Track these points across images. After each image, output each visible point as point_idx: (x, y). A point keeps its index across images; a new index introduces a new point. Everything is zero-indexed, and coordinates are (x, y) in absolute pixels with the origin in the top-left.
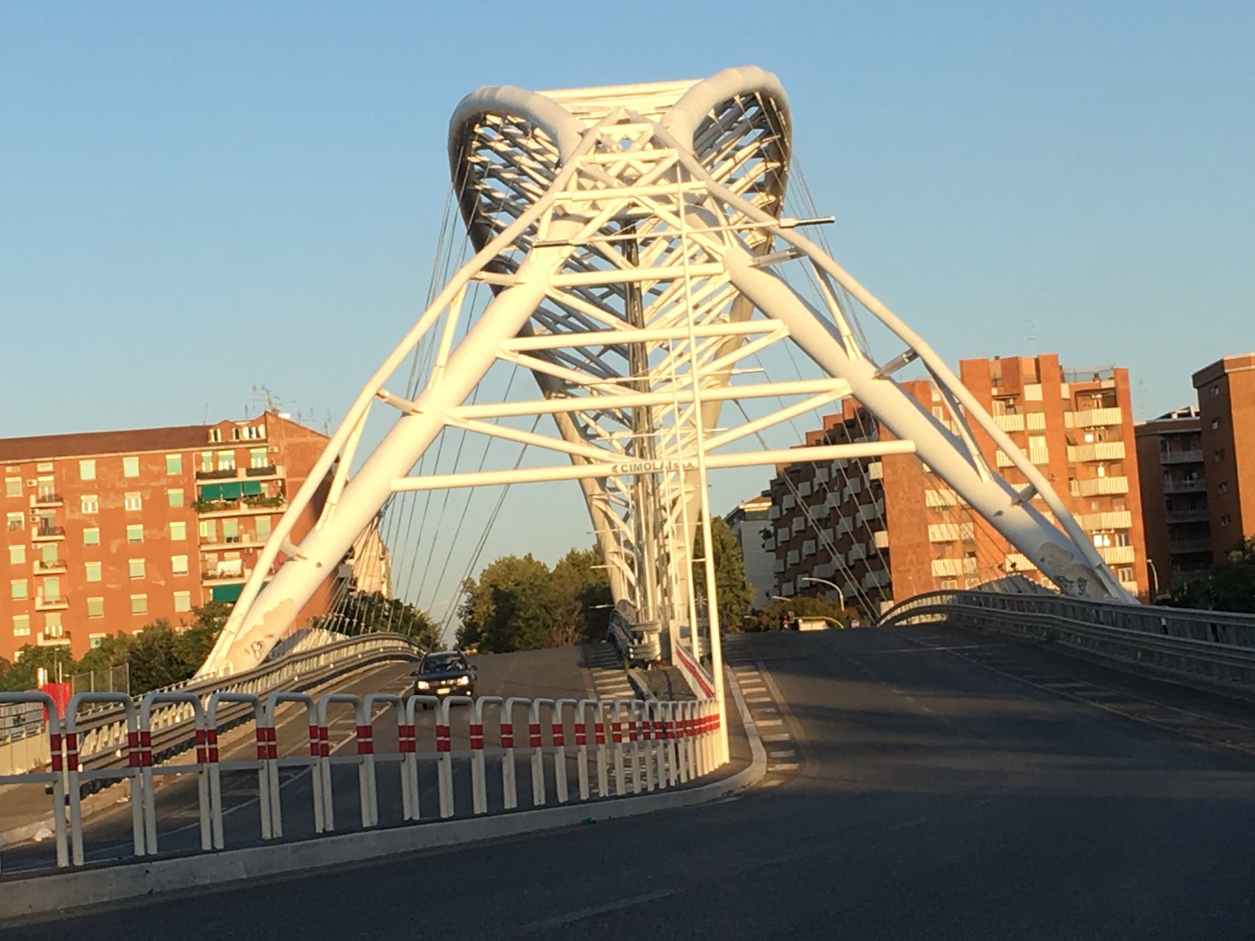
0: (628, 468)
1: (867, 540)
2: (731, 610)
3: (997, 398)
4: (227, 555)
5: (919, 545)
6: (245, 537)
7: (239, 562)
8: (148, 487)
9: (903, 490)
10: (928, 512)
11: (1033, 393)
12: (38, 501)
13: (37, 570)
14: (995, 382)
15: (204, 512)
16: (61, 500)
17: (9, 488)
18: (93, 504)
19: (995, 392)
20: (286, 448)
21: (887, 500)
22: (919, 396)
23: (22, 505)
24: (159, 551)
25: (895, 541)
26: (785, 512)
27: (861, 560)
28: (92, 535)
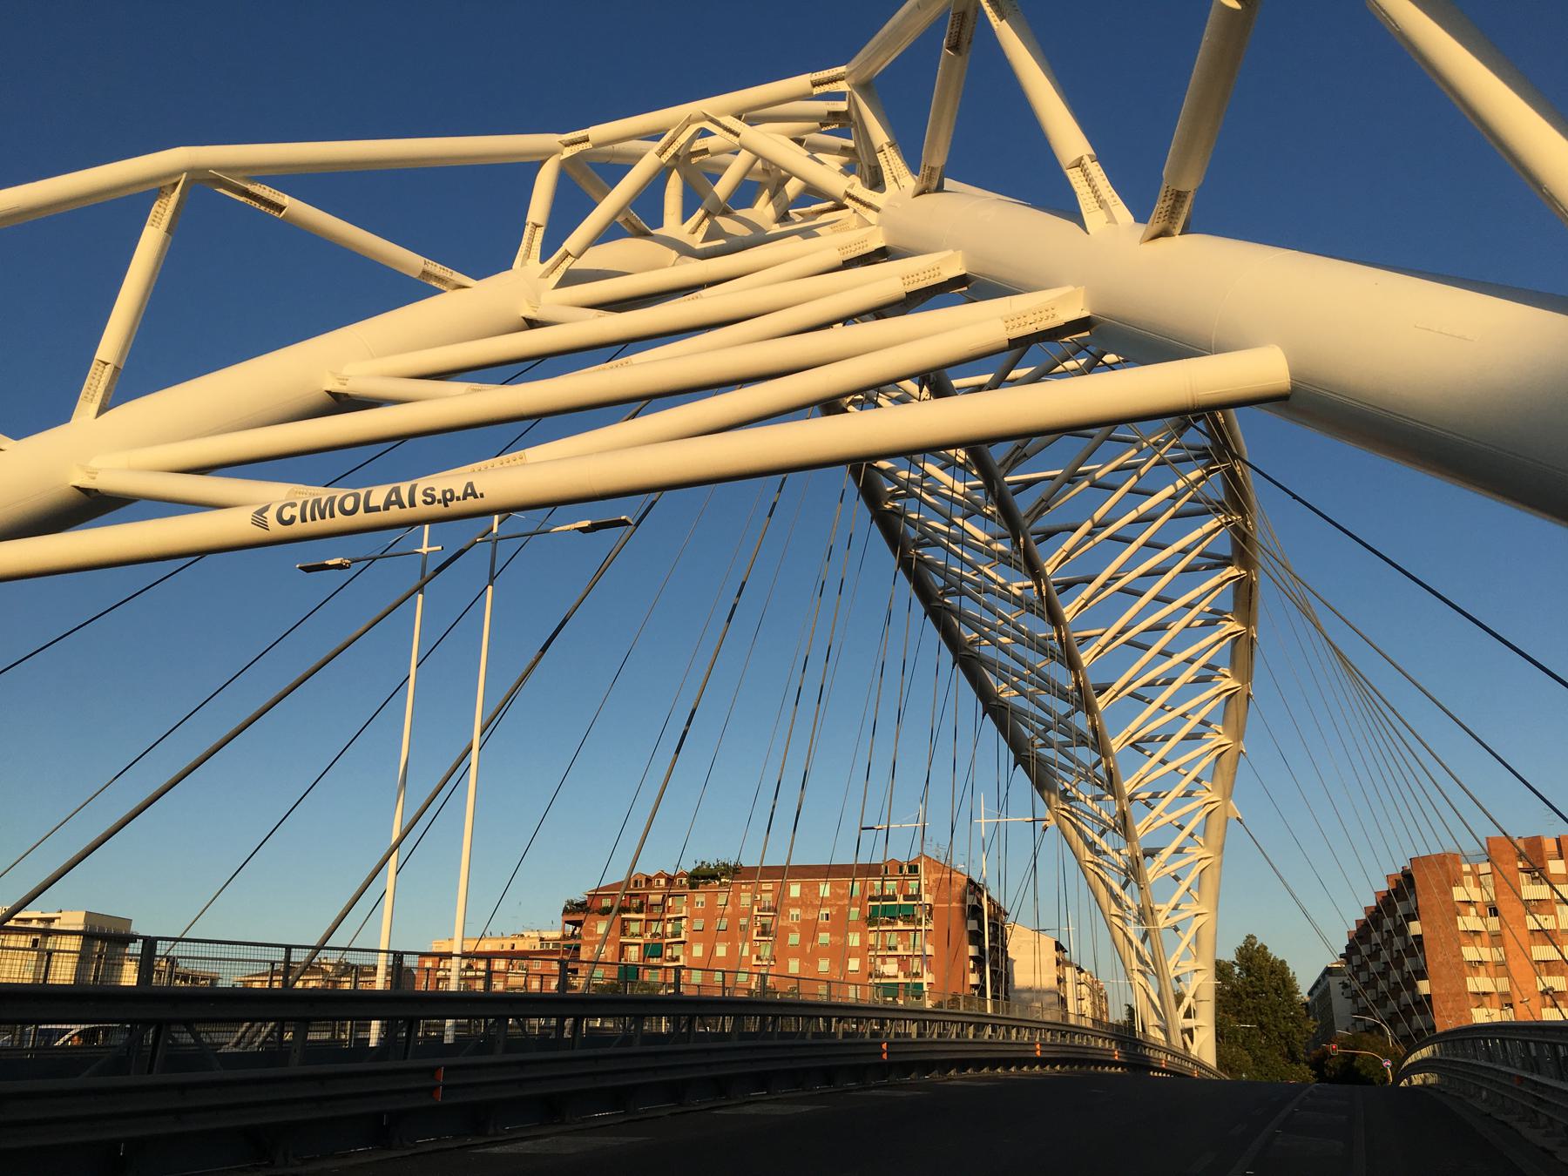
0: (297, 512)
1: (1413, 987)
2: (1293, 1039)
3: (1523, 870)
4: (888, 960)
5: (1458, 994)
6: (900, 947)
7: (897, 965)
8: (836, 905)
9: (1442, 945)
10: (1465, 966)
11: (1556, 867)
12: (758, 911)
13: (754, 962)
14: (1521, 856)
15: (873, 926)
16: (775, 911)
17: (742, 899)
18: (797, 916)
19: (1520, 865)
20: (934, 882)
21: (1426, 954)
22: (1450, 866)
23: (748, 913)
24: (840, 953)
25: (1436, 990)
26: (1355, 969)
27: (1385, 992)
28: (794, 939)
